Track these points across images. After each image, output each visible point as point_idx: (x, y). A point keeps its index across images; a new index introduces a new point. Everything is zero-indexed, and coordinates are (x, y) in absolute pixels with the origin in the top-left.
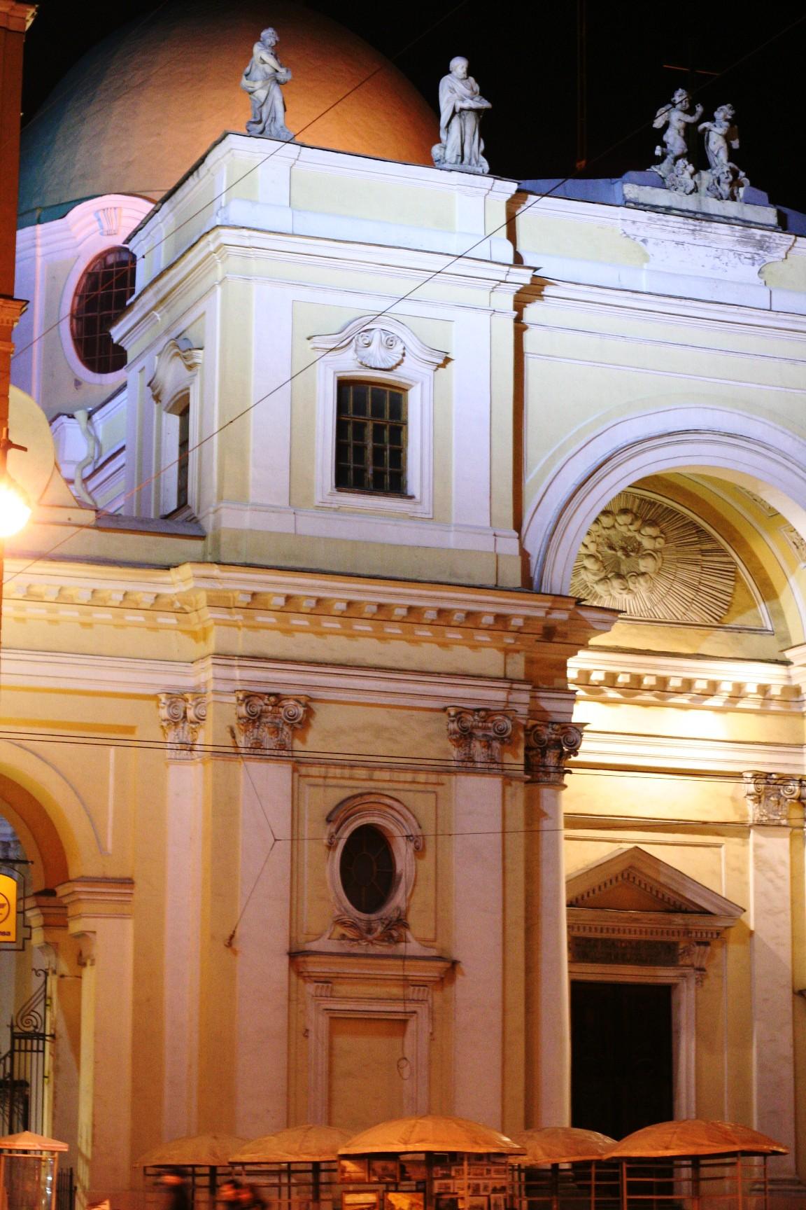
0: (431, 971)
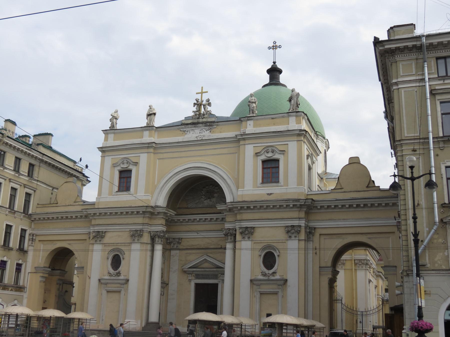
0: (124, 282)
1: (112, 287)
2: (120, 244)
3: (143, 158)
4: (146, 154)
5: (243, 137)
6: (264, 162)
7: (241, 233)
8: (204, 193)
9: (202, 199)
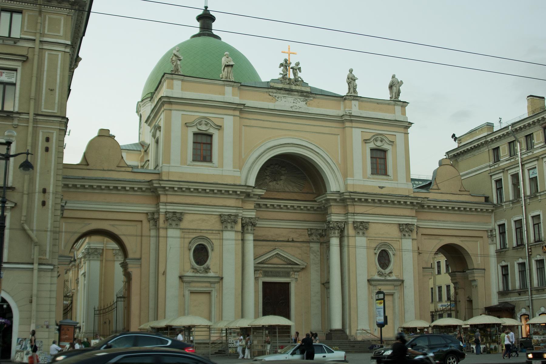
0: (217, 280)
1: (198, 287)
2: (205, 232)
3: (229, 122)
4: (232, 117)
5: (352, 119)
6: (372, 150)
7: (355, 228)
8: (268, 174)
9: (266, 180)
